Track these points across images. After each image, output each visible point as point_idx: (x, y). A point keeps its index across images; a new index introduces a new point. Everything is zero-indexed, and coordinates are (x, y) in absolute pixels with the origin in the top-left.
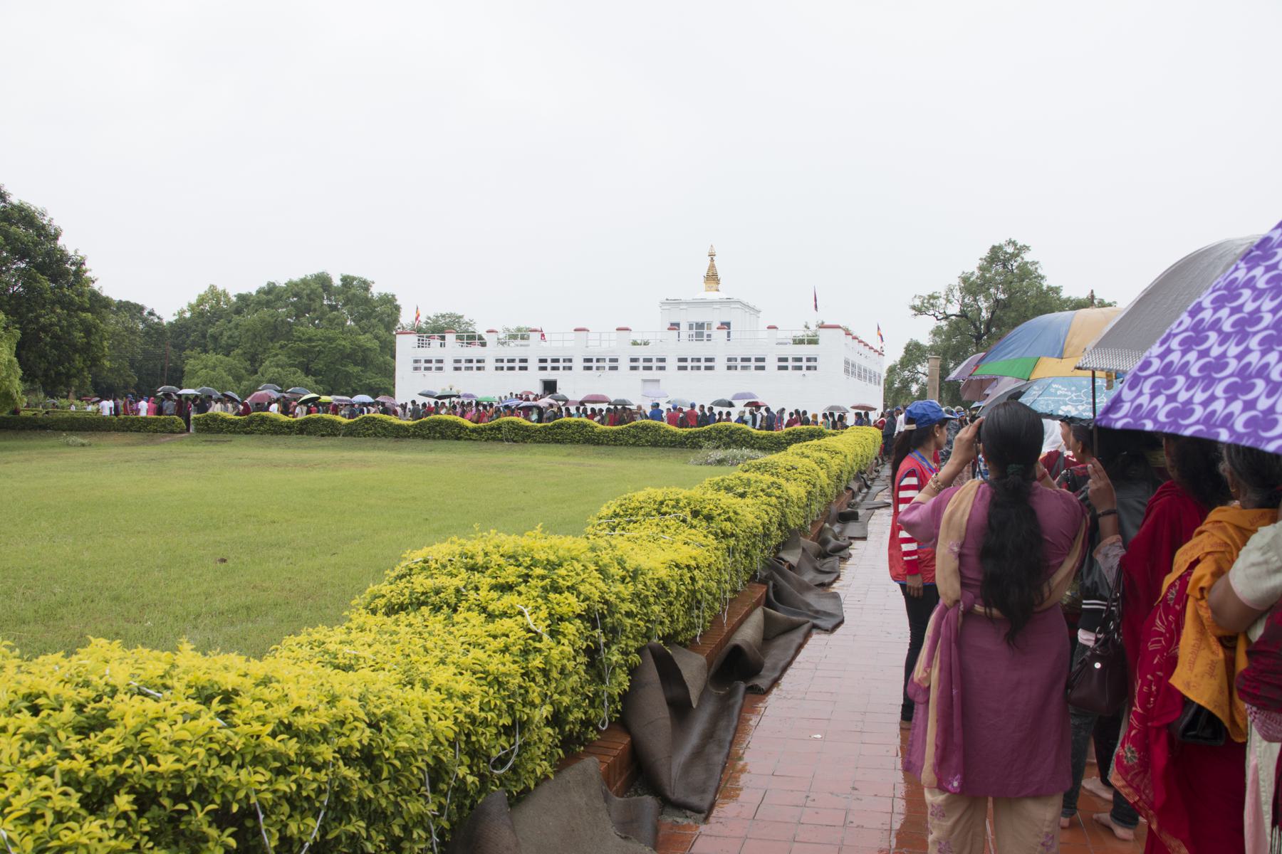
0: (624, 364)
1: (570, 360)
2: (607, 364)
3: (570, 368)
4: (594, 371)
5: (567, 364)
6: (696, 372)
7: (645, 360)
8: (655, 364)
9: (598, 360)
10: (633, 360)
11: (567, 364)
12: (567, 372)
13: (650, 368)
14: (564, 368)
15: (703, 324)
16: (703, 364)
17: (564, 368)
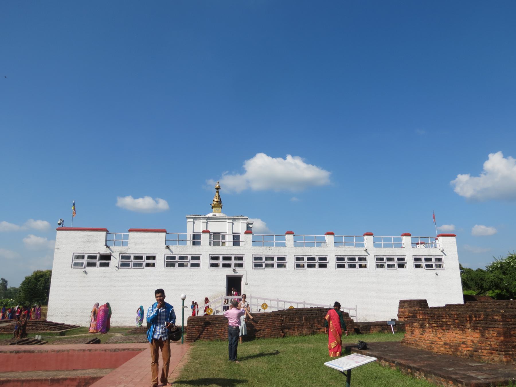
0: (205, 261)
4: (177, 269)
7: (225, 258)
8: (233, 262)
9: (181, 258)
10: (213, 258)
11: (151, 261)
13: (229, 266)
16: (275, 262)
17: (148, 265)
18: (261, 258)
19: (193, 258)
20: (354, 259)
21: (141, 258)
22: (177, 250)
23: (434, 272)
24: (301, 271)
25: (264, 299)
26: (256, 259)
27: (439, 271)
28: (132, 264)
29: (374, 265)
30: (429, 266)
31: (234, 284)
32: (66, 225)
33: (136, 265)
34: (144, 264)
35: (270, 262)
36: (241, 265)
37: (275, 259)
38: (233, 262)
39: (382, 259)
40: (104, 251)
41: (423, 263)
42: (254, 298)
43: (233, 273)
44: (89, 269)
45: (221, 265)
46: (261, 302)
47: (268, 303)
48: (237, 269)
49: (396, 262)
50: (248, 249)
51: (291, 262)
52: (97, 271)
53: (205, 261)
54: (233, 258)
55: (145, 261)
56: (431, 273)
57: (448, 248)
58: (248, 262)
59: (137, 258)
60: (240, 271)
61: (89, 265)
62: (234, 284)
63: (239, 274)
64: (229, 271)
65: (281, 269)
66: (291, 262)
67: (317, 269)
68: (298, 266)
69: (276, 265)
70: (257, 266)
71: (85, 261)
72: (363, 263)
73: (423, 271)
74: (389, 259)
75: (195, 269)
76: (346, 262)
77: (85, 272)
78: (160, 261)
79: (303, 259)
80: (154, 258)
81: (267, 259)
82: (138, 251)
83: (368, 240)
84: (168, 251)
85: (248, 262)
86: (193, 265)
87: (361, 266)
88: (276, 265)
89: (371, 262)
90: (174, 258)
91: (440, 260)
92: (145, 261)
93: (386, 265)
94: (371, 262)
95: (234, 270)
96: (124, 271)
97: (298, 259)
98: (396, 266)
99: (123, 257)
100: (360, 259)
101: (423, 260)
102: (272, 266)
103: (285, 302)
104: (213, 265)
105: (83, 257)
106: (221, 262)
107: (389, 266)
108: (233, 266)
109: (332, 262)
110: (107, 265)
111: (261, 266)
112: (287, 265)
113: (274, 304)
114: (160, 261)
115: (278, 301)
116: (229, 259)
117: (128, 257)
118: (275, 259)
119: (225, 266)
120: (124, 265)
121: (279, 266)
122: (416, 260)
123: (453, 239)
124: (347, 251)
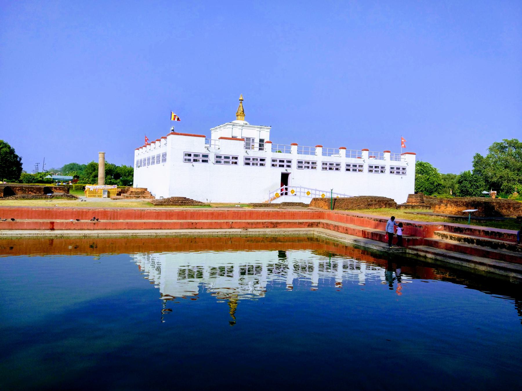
0: (268, 163)
1: (236, 158)
2: (251, 162)
3: (236, 163)
5: (235, 161)
6: (306, 170)
7: (280, 161)
8: (285, 164)
9: (253, 159)
10: (273, 161)
11: (235, 161)
12: (234, 165)
13: (283, 166)
14: (233, 163)
15: (250, 139)
17: (233, 163)
18: (301, 162)
19: (261, 160)
20: (356, 166)
21: (228, 158)
23: (400, 176)
24: (325, 172)
25: (308, 189)
26: (299, 162)
27: (403, 176)
28: (223, 161)
29: (367, 171)
30: (398, 173)
31: (285, 178)
32: (176, 131)
33: (225, 162)
34: (231, 162)
35: (307, 165)
36: (289, 166)
37: (310, 163)
38: (285, 164)
39: (372, 167)
40: (205, 151)
41: (395, 171)
42: (303, 187)
43: (285, 172)
44: (195, 164)
45: (278, 166)
46: (306, 191)
47: (310, 191)
48: (288, 169)
49: (380, 169)
50: (294, 155)
51: (319, 166)
52: (199, 165)
54: (285, 161)
55: (231, 160)
56: (399, 177)
57: (410, 162)
58: (294, 164)
59: (226, 158)
60: (289, 170)
61: (195, 160)
62: (285, 178)
63: (289, 171)
64: (283, 170)
65: (313, 170)
66: (319, 166)
68: (323, 168)
69: (310, 167)
70: (300, 167)
71: (192, 158)
72: (360, 168)
73: (394, 176)
74: (376, 167)
75: (262, 167)
76: (351, 168)
77: (193, 166)
78: (241, 161)
79: (326, 164)
80: (236, 158)
81: (305, 162)
82: (227, 154)
83: (365, 154)
84: (246, 155)
85: (294, 164)
86: (262, 165)
87: (359, 171)
88: (310, 167)
89: (366, 168)
90: (249, 159)
91: (404, 169)
92: (231, 160)
93: (374, 171)
94: (366, 168)
95: (286, 170)
96: (218, 165)
97: (323, 164)
98: (380, 171)
99: (217, 157)
100: (359, 166)
101: (395, 169)
102: (308, 167)
103: (319, 191)
104: (273, 165)
105: (190, 155)
106: (278, 163)
107: (375, 171)
108: (285, 166)
110: (206, 161)
111: (302, 167)
112: (317, 167)
113: (314, 192)
114: (241, 161)
115: (316, 190)
116: (283, 161)
117: (220, 157)
118: (310, 163)
119: (280, 166)
121: (312, 168)
122: (392, 168)
123: (414, 156)
124: (353, 161)
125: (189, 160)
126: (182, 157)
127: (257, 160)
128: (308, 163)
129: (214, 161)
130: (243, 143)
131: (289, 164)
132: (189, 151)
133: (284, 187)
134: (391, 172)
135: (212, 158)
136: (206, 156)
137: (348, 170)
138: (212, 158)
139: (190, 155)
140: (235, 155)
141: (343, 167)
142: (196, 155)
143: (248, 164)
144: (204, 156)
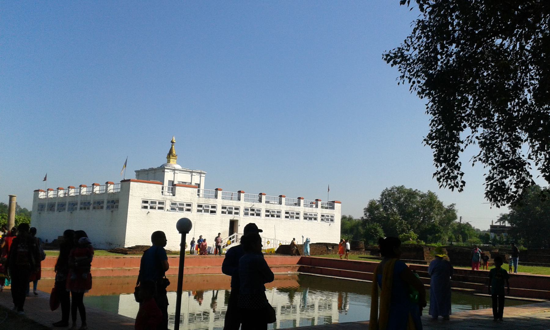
0: (219, 210)
5: (188, 208)
8: (234, 211)
18: (248, 210)
19: (213, 207)
22: (202, 201)
27: (332, 223)
35: (252, 212)
39: (306, 214)
48: (236, 215)
53: (219, 210)
58: (242, 212)
61: (151, 208)
63: (235, 219)
65: (258, 217)
67: (275, 218)
73: (323, 223)
85: (242, 212)
86: (212, 212)
99: (173, 204)
102: (253, 215)
109: (283, 215)
117: (175, 204)
119: (230, 213)
120: (173, 209)
125: (146, 207)
126: (141, 204)
127: (208, 207)
128: (253, 210)
129: (169, 208)
130: (196, 190)
131: (236, 211)
132: (146, 198)
133: (235, 234)
134: (322, 220)
135: (168, 206)
136: (162, 203)
137: (286, 217)
138: (168, 206)
139: (146, 202)
140: (189, 202)
141: (283, 215)
142: (152, 202)
143: (201, 211)
144: (160, 203)
